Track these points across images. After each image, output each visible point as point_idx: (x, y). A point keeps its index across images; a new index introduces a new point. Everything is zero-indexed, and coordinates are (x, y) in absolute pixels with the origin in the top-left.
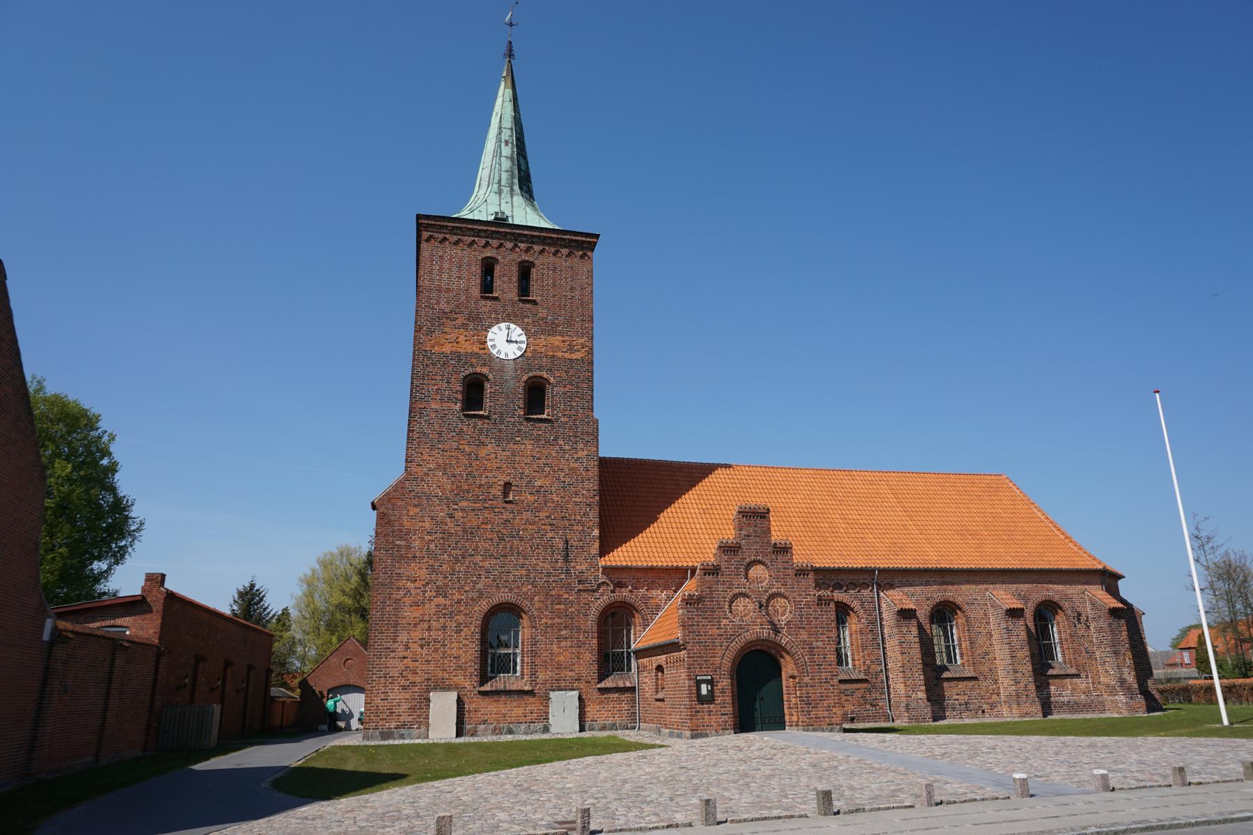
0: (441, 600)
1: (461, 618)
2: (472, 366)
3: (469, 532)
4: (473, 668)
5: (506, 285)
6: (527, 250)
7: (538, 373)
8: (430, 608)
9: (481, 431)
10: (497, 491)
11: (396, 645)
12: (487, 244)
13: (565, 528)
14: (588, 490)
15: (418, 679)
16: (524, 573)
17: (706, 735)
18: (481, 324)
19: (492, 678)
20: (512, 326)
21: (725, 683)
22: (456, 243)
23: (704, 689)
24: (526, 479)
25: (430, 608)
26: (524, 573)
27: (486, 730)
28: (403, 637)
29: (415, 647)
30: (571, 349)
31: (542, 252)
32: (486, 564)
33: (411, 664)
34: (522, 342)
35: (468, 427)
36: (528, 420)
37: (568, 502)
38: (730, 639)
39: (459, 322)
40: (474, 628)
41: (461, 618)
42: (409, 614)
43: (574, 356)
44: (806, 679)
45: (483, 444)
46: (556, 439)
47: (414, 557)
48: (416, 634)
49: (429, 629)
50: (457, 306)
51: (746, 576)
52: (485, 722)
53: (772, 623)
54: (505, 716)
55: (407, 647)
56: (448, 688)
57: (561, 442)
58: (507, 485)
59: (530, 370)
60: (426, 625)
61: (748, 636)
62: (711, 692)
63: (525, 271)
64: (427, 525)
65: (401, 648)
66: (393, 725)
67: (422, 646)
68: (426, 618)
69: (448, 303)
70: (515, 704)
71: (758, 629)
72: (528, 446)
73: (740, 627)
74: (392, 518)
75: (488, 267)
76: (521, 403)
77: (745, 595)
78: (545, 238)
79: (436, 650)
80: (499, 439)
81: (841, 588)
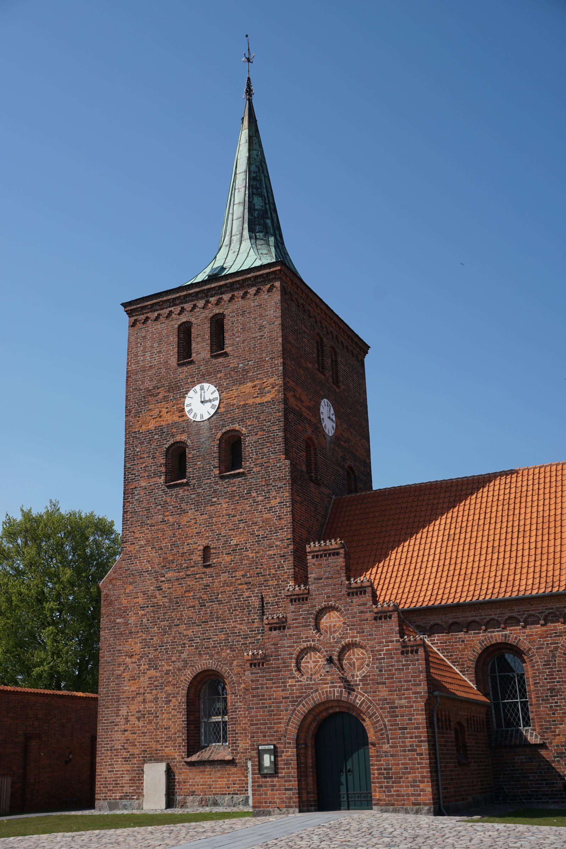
0: (152, 672)
1: (169, 689)
2: (173, 436)
3: (176, 602)
4: (181, 738)
5: (201, 348)
6: (218, 303)
7: (232, 427)
8: (144, 681)
9: (182, 499)
10: (197, 557)
11: (118, 719)
12: (183, 310)
13: (261, 585)
14: (282, 540)
15: (136, 751)
16: (223, 637)
17: (269, 814)
18: (179, 391)
19: (204, 747)
20: (206, 385)
21: (289, 753)
22: (157, 319)
23: (267, 760)
24: (223, 540)
25: (144, 681)
26: (223, 637)
27: (193, 801)
28: (124, 711)
29: (133, 719)
30: (262, 393)
31: (232, 299)
32: (190, 633)
33: (131, 737)
34: (214, 399)
35: (171, 498)
36: (222, 478)
37: (262, 557)
38: (296, 701)
39: (160, 396)
40: (181, 699)
41: (169, 689)
42: (128, 688)
43: (265, 399)
44: (386, 747)
45: (184, 512)
46: (249, 493)
47: (131, 633)
48: (134, 708)
49: (144, 701)
50: (159, 381)
51: (317, 627)
52: (193, 793)
53: (344, 680)
54: (210, 786)
55: (127, 721)
56: (158, 760)
57: (254, 494)
58: (207, 549)
59: (224, 426)
60: (141, 699)
61: (316, 698)
62: (275, 763)
63: (218, 325)
64: (140, 600)
65: (123, 721)
66: (118, 795)
67: (138, 719)
68: (142, 691)
69: (151, 380)
70: (218, 774)
71: (327, 688)
72: (224, 505)
73: (308, 687)
74: (113, 598)
75: (185, 332)
76: (216, 462)
77: (314, 649)
78: (232, 284)
79: (150, 722)
80: (197, 504)
81: (517, 623)
